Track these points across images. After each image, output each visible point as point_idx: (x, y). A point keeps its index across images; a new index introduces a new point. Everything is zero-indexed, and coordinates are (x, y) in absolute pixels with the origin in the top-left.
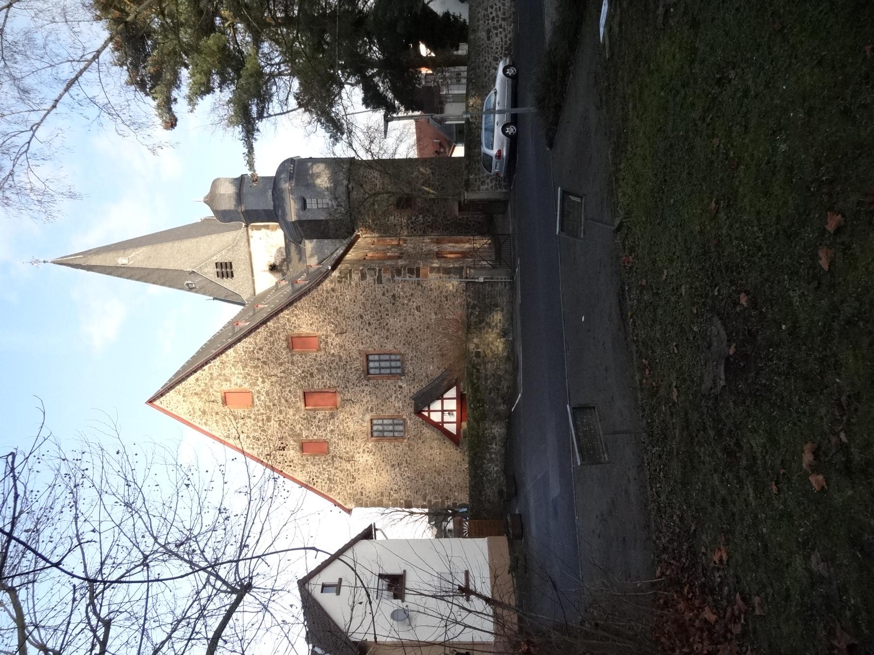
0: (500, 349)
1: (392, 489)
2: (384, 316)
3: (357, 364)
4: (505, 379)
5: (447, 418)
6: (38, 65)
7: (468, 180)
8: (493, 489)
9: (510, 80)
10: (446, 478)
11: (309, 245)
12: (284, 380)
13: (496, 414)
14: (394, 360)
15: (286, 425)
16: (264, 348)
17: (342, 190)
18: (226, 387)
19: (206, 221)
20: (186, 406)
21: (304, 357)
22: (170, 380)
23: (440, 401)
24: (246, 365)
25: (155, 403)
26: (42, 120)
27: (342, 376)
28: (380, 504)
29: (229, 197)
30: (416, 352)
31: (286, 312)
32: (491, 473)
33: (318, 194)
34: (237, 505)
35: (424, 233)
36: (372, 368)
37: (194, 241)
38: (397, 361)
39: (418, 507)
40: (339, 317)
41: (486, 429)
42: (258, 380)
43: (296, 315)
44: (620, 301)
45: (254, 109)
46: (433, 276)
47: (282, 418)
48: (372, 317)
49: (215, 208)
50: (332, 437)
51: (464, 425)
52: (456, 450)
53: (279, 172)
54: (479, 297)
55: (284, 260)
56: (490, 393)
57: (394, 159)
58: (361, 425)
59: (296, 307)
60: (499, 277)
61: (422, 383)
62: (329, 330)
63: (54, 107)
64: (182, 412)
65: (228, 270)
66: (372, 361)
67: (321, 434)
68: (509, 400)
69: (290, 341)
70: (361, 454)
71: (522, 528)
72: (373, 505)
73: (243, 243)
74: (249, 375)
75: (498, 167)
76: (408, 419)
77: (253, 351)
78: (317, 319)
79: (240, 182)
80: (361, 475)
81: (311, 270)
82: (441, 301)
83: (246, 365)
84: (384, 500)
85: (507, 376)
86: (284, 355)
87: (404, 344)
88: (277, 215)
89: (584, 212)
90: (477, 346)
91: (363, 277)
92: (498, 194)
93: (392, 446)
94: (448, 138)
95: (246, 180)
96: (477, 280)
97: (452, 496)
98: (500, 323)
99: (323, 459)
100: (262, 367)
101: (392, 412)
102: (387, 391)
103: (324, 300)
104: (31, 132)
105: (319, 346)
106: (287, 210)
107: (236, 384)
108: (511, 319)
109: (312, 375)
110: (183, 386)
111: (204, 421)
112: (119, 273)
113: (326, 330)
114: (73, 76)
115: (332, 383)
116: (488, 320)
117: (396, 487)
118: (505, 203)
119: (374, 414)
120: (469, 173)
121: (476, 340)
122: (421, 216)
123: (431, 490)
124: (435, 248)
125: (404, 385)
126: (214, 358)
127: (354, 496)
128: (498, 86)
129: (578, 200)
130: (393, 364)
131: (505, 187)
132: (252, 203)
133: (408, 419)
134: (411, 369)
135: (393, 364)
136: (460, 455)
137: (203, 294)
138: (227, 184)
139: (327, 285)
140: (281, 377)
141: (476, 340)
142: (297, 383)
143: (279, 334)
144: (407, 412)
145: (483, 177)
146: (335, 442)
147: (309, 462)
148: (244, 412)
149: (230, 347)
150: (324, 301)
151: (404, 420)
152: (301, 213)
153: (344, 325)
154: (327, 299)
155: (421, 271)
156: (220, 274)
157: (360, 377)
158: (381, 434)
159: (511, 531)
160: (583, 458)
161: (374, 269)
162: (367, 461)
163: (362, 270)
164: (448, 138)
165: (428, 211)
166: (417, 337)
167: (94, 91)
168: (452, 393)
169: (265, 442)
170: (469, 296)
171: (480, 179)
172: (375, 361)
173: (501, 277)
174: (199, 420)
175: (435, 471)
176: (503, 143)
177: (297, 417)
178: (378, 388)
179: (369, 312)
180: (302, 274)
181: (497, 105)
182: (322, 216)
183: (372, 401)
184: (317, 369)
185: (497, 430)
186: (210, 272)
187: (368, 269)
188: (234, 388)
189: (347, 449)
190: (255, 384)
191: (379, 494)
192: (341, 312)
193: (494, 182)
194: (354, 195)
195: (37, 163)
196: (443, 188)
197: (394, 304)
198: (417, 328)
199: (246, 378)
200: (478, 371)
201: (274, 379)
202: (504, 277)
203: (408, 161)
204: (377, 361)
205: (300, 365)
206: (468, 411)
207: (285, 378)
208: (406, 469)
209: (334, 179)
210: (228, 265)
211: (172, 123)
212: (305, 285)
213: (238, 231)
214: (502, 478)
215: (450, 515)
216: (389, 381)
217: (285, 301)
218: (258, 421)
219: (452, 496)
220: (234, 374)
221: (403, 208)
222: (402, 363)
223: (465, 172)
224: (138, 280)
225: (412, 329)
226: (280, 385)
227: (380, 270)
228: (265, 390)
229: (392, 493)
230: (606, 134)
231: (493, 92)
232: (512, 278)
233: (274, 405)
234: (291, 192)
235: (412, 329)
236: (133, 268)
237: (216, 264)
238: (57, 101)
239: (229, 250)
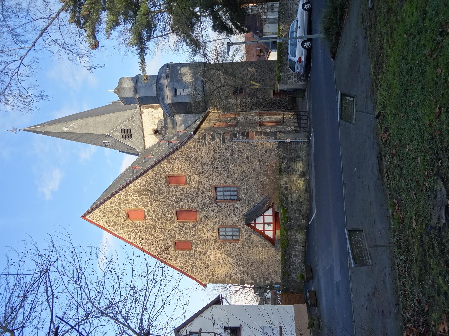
0: (301, 185)
1: (232, 273)
2: (226, 163)
3: (209, 193)
4: (304, 204)
5: (267, 228)
6: (24, 21)
7: (280, 77)
8: (297, 274)
9: (307, 12)
10: (266, 266)
11: (179, 118)
12: (164, 203)
13: (298, 226)
14: (233, 191)
15: (166, 231)
16: (152, 184)
17: (199, 83)
18: (129, 207)
19: (115, 103)
20: (104, 219)
21: (176, 189)
22: (95, 203)
23: (262, 217)
24: (141, 194)
25: (86, 217)
26: (27, 54)
27: (200, 200)
28: (224, 282)
29: (130, 88)
30: (247, 186)
31: (165, 161)
32: (295, 264)
33: (185, 86)
34: (140, 283)
35: (252, 109)
36: (219, 196)
37: (108, 116)
38: (234, 191)
39: (248, 284)
40: (198, 164)
41: (292, 236)
42: (148, 203)
43: (171, 163)
44: (379, 161)
45: (145, 34)
46: (257, 138)
47: (163, 227)
48: (218, 164)
49: (121, 96)
50: (194, 239)
51: (278, 232)
52: (273, 248)
53: (160, 73)
54: (287, 152)
55: (163, 127)
56: (295, 213)
57: (233, 63)
58: (212, 231)
59: (171, 158)
60: (300, 139)
61: (251, 205)
62: (191, 172)
63: (34, 46)
64: (102, 223)
65: (129, 134)
66: (219, 191)
67: (187, 237)
68: (307, 217)
70: (212, 250)
71: (316, 300)
72: (220, 282)
73: (138, 117)
74: (142, 200)
75: (299, 68)
76: (242, 228)
77: (145, 185)
78: (184, 165)
79: (136, 79)
80: (212, 263)
81: (180, 134)
82: (262, 153)
83: (141, 194)
84: (227, 279)
85: (305, 202)
86: (164, 188)
87: (239, 181)
88: (159, 100)
89: (356, 106)
90: (286, 183)
91: (213, 138)
92: (299, 85)
93: (232, 245)
94: (266, 46)
95: (140, 79)
96: (285, 141)
97: (270, 278)
98: (301, 168)
99: (188, 253)
100: (151, 195)
101: (232, 223)
102: (228, 210)
103: (189, 153)
104: (20, 61)
105: (186, 182)
106: (166, 97)
107: (135, 206)
108: (308, 165)
109: (181, 200)
110: (103, 206)
111: (115, 228)
112: (64, 136)
113: (190, 172)
114: (44, 28)
115: (194, 205)
116: (293, 166)
117: (235, 271)
118: (303, 91)
119: (220, 224)
120: (280, 72)
121: (285, 179)
122: (249, 99)
123: (257, 273)
124: (258, 119)
125: (239, 207)
126: (121, 189)
127: (208, 276)
128: (299, 17)
129: (352, 99)
130: (232, 193)
131: (304, 81)
132: (143, 93)
133: (242, 228)
134: (243, 196)
135: (232, 193)
136: (275, 251)
137: (114, 149)
138: (128, 80)
139: (190, 144)
140: (162, 202)
141: (285, 179)
142: (172, 205)
143: (161, 175)
144: (241, 224)
145: (289, 75)
146: (196, 242)
147: (180, 255)
148: (140, 223)
149: (131, 182)
150: (189, 154)
151: (240, 229)
152: (174, 98)
153: (201, 169)
154: (190, 152)
155: (250, 135)
156: (124, 137)
157: (211, 201)
158: (225, 238)
159: (309, 302)
160: (355, 262)
161: (220, 134)
162: (216, 254)
163: (213, 134)
164: (266, 46)
165: (253, 95)
166: (247, 176)
167: (56, 36)
168: (270, 212)
169: (152, 242)
170: (281, 151)
171: (287, 76)
172: (221, 191)
173: (301, 138)
174: (112, 228)
175: (259, 261)
176: (302, 54)
177: (172, 226)
178: (222, 208)
179: (217, 161)
180: (174, 136)
181: (298, 28)
182: (187, 100)
183: (219, 217)
184: (184, 196)
185: (300, 237)
186: (118, 135)
187: (216, 134)
188: (133, 208)
189: (204, 247)
190: (146, 206)
191: (224, 275)
192: (199, 160)
193: (296, 78)
194: (207, 86)
195: (23, 78)
196: (263, 81)
197: (232, 155)
198: (247, 170)
199: (141, 202)
200: (287, 198)
201: (158, 203)
202: (303, 139)
203: (241, 64)
204: (222, 191)
205: (173, 194)
206: (281, 224)
207: (165, 202)
208: (241, 260)
209: (194, 76)
210: (129, 131)
211: (96, 45)
212: (176, 144)
213: (135, 109)
214: (303, 267)
215: (268, 289)
216: (229, 204)
217: (164, 154)
218: (148, 229)
219: (270, 278)
220: (134, 199)
221: (238, 94)
222: (238, 193)
223: (278, 72)
224: (75, 140)
225: (244, 171)
226: (162, 206)
227: (224, 134)
228: (153, 209)
229: (232, 275)
230: (369, 54)
231: (295, 20)
232: (308, 139)
233: (158, 219)
234: (168, 85)
235: (244, 171)
236: (72, 133)
237: (122, 130)
238: (35, 42)
239: (129, 121)
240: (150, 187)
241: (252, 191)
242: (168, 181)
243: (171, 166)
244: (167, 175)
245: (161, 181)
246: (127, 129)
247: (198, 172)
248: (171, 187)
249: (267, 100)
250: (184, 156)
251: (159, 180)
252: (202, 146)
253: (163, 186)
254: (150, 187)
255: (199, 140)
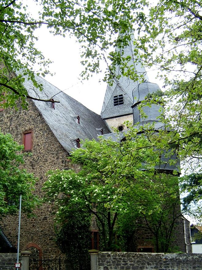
21: (20, 141)
40: (42, 163)
59: (49, 134)
69: (29, 132)
78: (41, 148)
96: (18, 262)
143: (33, 124)
153: (37, 167)
154: (53, 154)
192: (45, 164)
198: (33, 218)
201: (8, 124)
226: (6, 128)
237: (122, 95)
240: (23, 115)
241: (14, 223)
242: (27, 132)
243: (41, 134)
244: (32, 130)
245: (28, 126)
246: (122, 101)
247: (34, 163)
248: (21, 136)
249: (136, 241)
250: (49, 147)
251: (28, 123)
252: (58, 166)
253: (23, 127)
254: (23, 115)
255: (64, 162)
